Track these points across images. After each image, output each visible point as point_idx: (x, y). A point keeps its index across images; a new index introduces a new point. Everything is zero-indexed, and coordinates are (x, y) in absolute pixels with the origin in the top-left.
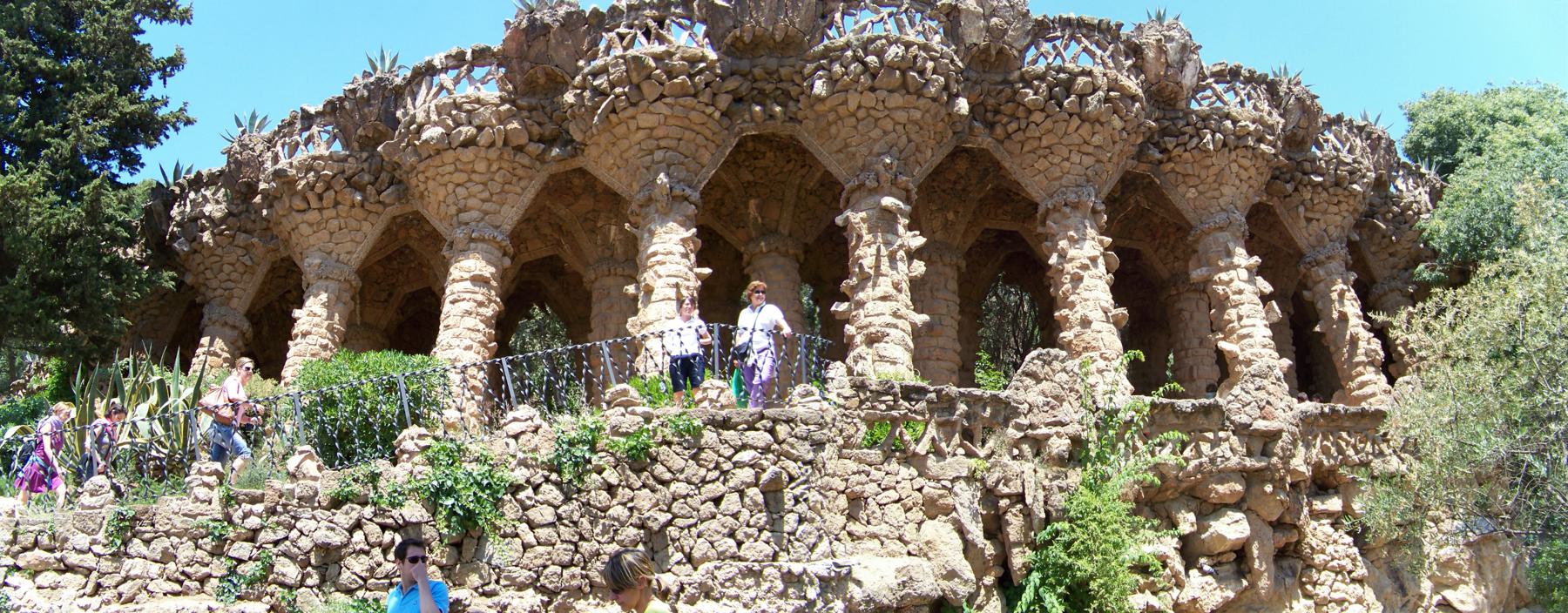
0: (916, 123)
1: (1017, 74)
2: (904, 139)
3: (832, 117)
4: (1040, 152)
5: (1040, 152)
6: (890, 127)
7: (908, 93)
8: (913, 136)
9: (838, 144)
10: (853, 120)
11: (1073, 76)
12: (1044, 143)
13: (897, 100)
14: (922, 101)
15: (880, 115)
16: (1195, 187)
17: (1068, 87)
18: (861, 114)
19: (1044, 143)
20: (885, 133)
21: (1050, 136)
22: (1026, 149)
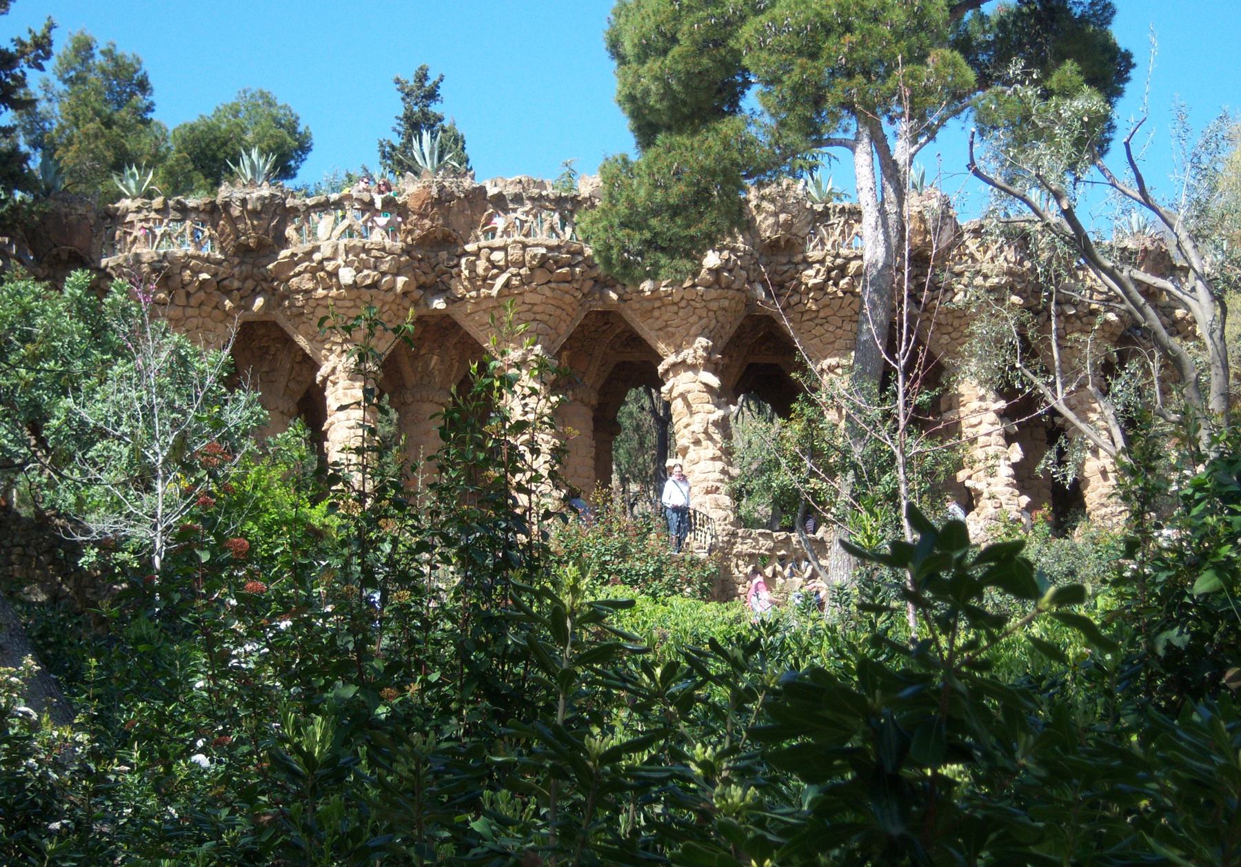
0: (724, 309)
1: (800, 257)
2: (714, 321)
3: (657, 304)
4: (818, 321)
5: (818, 321)
6: (704, 314)
7: (720, 287)
8: (720, 319)
9: (660, 323)
10: (675, 308)
11: (848, 260)
12: (822, 314)
13: (713, 293)
14: (731, 293)
15: (698, 305)
16: (949, 334)
17: (842, 270)
18: (683, 304)
19: (822, 314)
20: (700, 318)
21: (827, 309)
22: (805, 318)
